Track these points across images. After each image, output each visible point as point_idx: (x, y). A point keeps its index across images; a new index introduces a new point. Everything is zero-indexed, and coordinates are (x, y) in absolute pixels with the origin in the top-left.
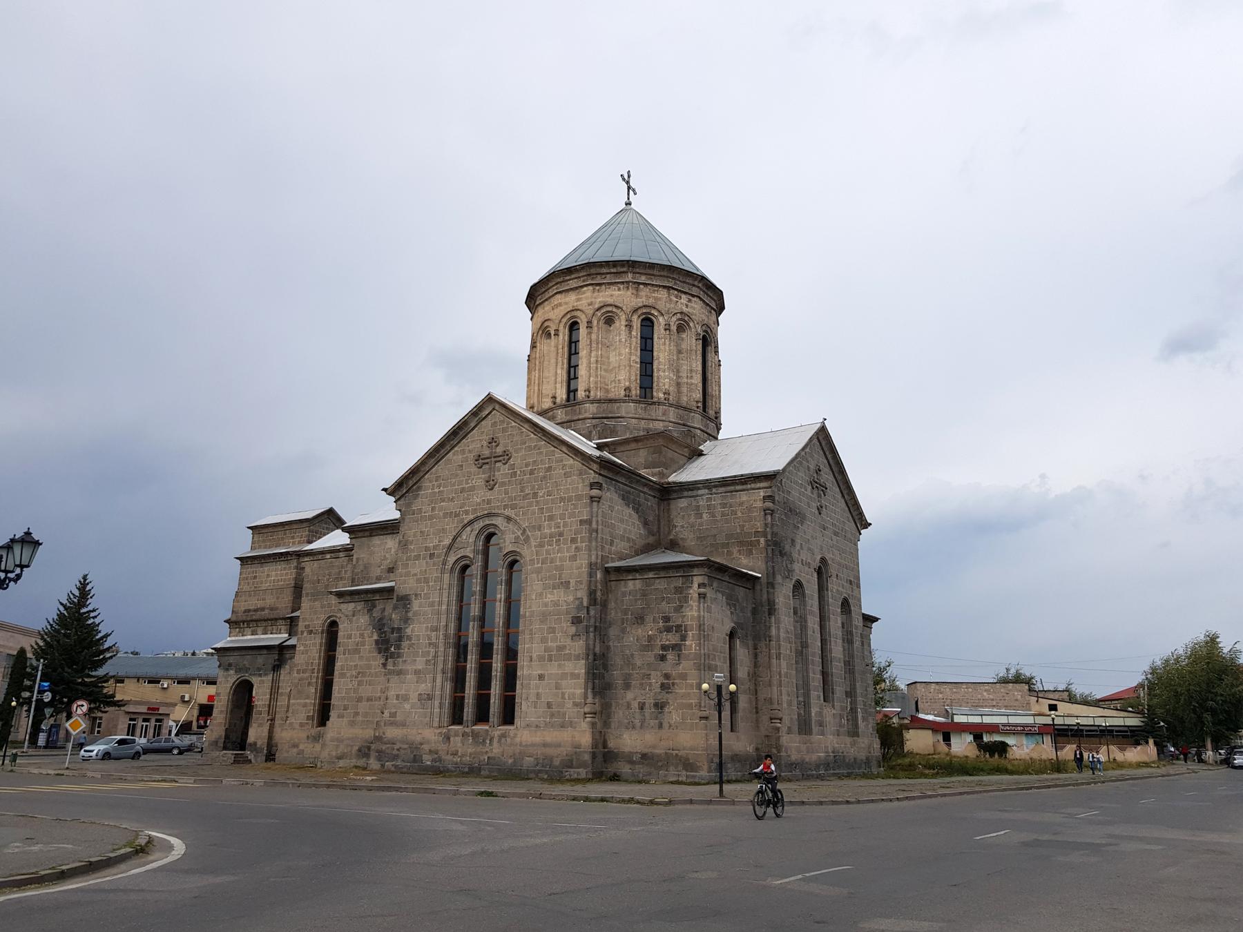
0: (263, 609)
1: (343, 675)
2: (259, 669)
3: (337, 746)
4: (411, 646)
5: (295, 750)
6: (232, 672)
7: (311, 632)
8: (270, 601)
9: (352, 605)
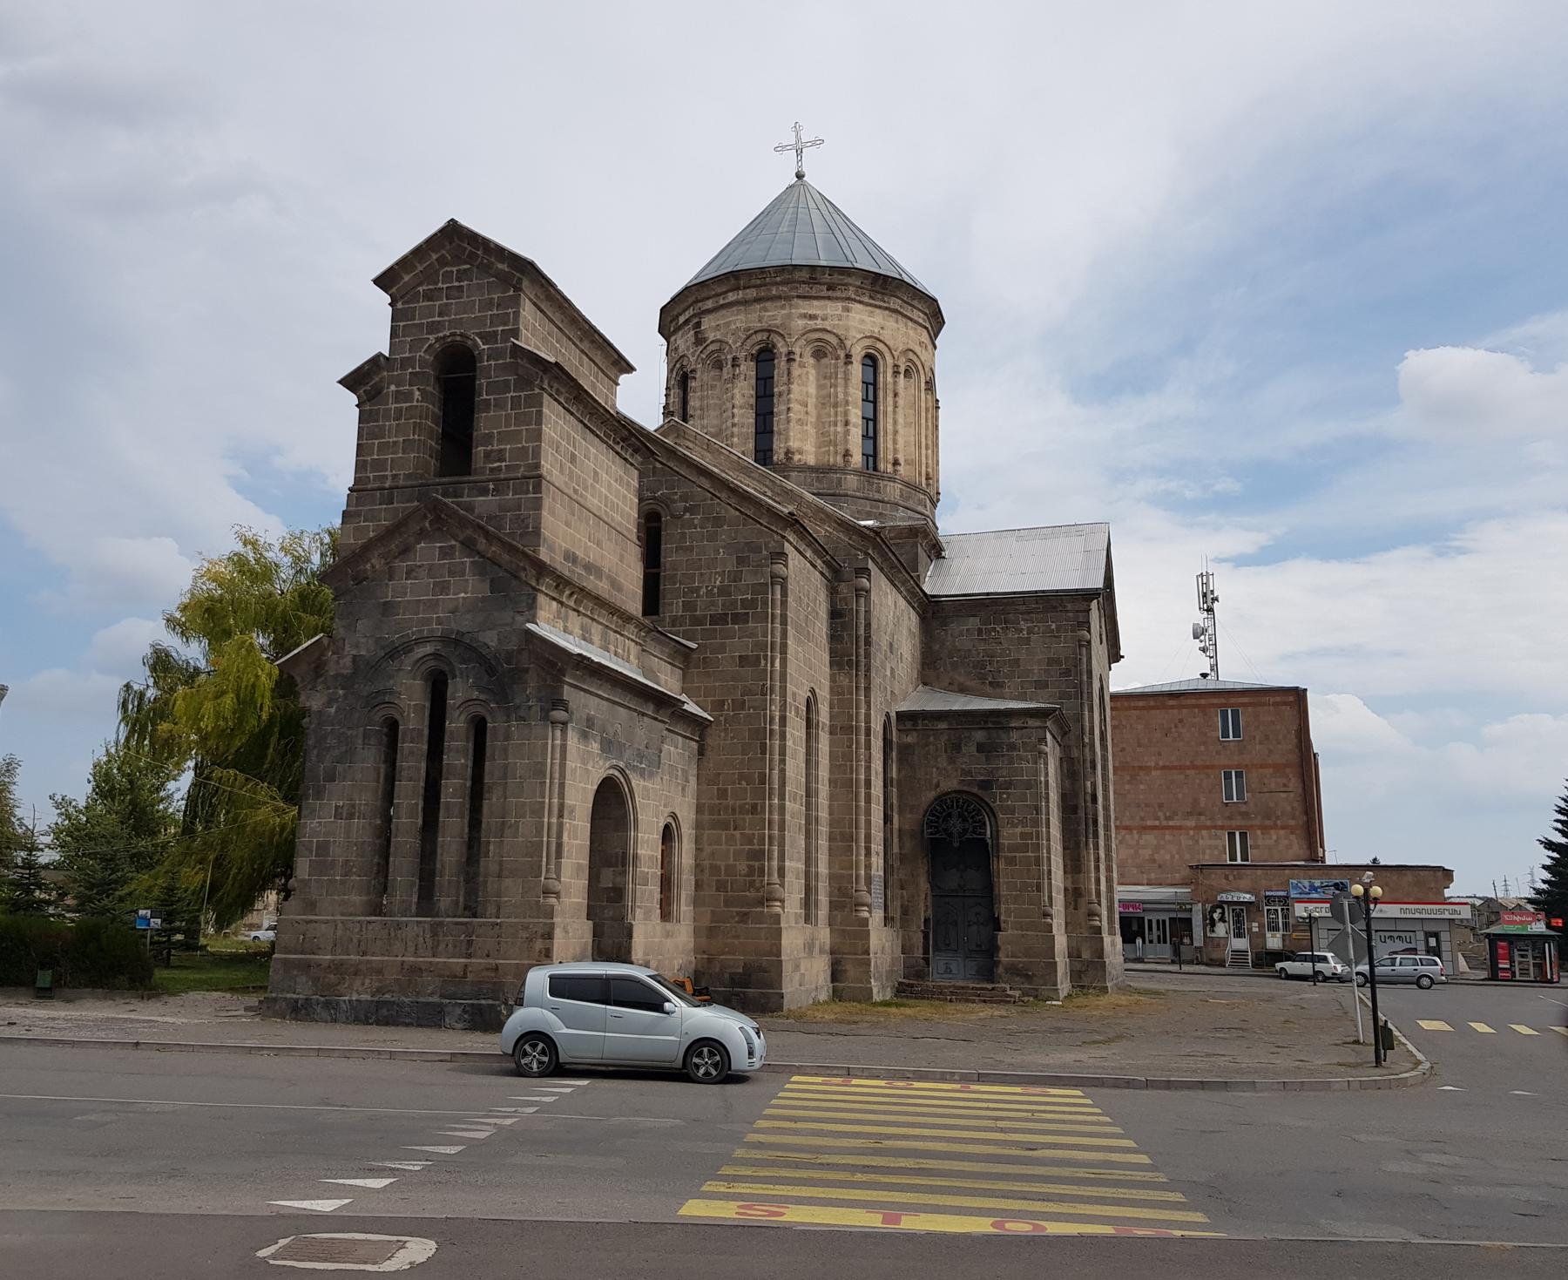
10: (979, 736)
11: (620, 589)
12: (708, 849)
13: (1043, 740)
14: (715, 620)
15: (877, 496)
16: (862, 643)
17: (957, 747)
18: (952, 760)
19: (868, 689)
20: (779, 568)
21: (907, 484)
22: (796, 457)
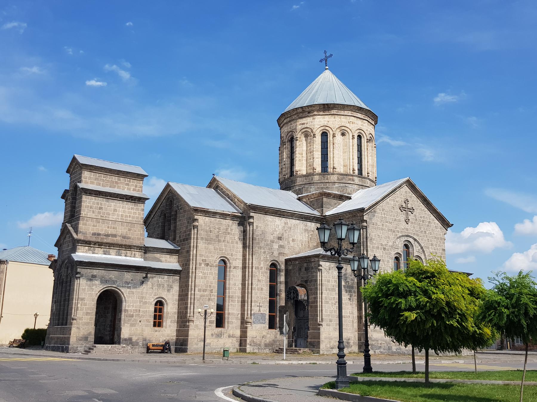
0: (115, 236)
1: (327, 302)
2: (128, 283)
3: (330, 342)
6: (97, 282)
7: (207, 265)
8: (121, 230)
9: (328, 264)
10: (305, 265)
14: (184, 240)
15: (326, 181)
17: (300, 269)
18: (299, 274)
20: (196, 224)
21: (342, 174)
22: (299, 173)
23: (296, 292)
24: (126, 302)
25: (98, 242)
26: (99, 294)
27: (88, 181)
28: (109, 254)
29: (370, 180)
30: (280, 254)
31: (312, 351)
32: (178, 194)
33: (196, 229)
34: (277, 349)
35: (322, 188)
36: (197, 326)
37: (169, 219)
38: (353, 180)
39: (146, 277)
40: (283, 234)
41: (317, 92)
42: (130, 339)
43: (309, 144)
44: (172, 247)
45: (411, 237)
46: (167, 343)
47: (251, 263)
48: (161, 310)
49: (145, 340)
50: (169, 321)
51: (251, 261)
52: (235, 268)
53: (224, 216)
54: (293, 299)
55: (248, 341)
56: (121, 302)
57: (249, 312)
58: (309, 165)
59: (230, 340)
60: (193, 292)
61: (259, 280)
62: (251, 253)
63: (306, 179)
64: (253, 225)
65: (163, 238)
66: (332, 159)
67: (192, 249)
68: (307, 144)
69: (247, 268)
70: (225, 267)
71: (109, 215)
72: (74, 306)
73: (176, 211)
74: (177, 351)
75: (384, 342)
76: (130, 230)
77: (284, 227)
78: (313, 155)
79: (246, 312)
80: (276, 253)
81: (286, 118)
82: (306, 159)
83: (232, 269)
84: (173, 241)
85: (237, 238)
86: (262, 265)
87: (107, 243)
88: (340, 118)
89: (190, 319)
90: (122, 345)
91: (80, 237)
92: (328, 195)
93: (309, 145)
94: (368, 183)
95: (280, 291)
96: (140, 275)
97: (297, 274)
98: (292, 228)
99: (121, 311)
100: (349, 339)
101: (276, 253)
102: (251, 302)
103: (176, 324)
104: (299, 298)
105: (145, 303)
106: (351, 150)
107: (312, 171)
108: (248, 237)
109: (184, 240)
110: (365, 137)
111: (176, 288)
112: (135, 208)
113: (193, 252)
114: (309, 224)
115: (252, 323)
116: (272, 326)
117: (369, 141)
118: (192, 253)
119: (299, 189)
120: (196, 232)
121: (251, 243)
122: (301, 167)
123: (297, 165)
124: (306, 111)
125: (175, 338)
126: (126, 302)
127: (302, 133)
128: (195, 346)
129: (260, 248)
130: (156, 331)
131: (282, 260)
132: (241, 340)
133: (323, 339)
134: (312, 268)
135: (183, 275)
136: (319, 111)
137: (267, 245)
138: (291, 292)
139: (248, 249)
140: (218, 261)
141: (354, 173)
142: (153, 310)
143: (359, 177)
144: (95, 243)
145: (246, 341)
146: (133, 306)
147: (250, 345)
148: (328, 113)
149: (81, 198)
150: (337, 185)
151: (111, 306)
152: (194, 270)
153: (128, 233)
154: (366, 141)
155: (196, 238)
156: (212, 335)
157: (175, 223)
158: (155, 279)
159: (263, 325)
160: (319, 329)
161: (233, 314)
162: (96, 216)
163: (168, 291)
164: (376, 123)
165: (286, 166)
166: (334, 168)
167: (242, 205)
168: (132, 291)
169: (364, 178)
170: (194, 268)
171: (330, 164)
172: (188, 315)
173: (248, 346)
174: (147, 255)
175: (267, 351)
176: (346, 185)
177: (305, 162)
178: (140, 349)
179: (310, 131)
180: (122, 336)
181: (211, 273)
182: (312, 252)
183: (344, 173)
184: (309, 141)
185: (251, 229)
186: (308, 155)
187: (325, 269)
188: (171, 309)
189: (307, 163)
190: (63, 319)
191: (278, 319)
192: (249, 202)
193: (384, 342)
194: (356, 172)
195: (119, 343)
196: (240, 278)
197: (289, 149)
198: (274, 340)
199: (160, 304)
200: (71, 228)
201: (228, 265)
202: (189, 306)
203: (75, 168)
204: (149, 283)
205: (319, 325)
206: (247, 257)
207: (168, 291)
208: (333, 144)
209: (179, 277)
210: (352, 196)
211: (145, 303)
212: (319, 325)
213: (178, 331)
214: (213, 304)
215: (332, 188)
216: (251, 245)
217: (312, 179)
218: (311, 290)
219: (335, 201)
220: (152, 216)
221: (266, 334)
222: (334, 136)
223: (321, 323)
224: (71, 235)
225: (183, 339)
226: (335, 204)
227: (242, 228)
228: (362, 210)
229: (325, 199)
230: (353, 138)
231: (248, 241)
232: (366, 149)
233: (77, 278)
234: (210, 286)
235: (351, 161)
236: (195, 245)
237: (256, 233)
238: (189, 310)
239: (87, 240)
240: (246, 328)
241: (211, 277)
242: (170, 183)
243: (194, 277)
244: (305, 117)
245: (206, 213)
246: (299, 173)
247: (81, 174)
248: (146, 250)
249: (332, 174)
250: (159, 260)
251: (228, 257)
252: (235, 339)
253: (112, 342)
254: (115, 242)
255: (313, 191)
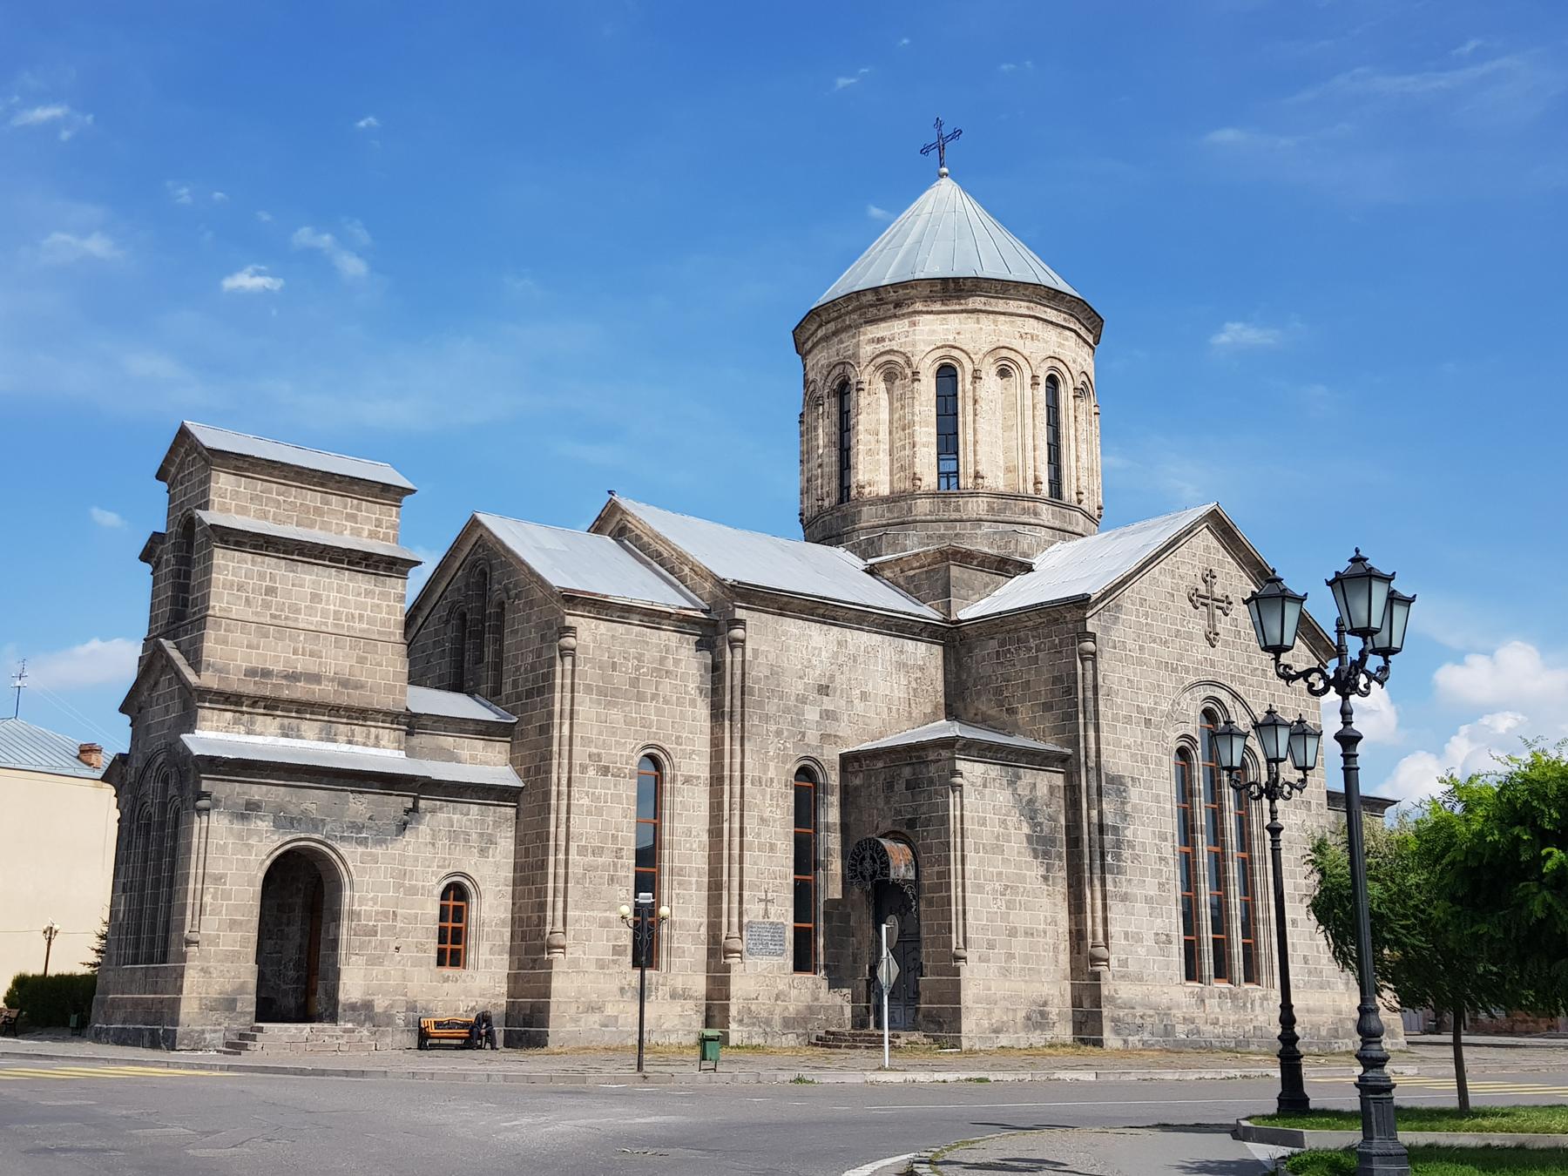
0: (315, 678)
1: (979, 888)
2: (359, 828)
3: (990, 1012)
4: (1135, 858)
5: (595, 1018)
7: (605, 771)
8: (335, 660)
10: (907, 772)
11: (359, 686)
12: (519, 902)
13: (955, 773)
14: (529, 694)
15: (955, 516)
16: (738, 693)
19: (742, 738)
20: (569, 641)
21: (1001, 496)
22: (866, 491)
23: (882, 857)
24: (352, 888)
25: (265, 698)
26: (268, 863)
27: (230, 503)
28: (299, 737)
29: (1084, 513)
30: (825, 737)
31: (936, 1040)
32: (508, 551)
33: (568, 660)
34: (822, 1033)
35: (942, 537)
36: (575, 963)
37: (480, 626)
38: (1036, 514)
39: (415, 809)
40: (832, 677)
41: (919, 242)
42: (368, 1006)
43: (899, 402)
44: (490, 716)
45: (1222, 686)
46: (484, 1018)
47: (737, 767)
48: (459, 915)
49: (412, 1007)
50: (485, 947)
51: (737, 760)
52: (687, 780)
53: (653, 617)
54: (872, 877)
55: (733, 1011)
56: (338, 887)
57: (735, 919)
58: (903, 467)
59: (677, 1007)
60: (561, 856)
61: (763, 820)
62: (737, 735)
63: (890, 510)
64: (743, 648)
65: (457, 687)
66: (970, 448)
67: (557, 721)
68: (891, 403)
69: (727, 781)
70: (659, 780)
71: (298, 611)
72: (190, 901)
73: (501, 604)
74: (512, 1042)
75: (1151, 1012)
76: (361, 660)
77: (835, 655)
78: (912, 435)
79: (725, 920)
80: (812, 737)
81: (824, 323)
82: (888, 446)
83: (679, 784)
84: (493, 696)
85: (692, 687)
86: (771, 773)
87: (292, 702)
88: (995, 322)
89: (555, 942)
90: (342, 1025)
91: (208, 680)
92: (965, 558)
93: (897, 405)
94: (1080, 523)
95: (827, 852)
96: (397, 803)
97: (881, 803)
98: (860, 659)
99: (336, 918)
100: (1045, 1004)
101: (812, 737)
102: (741, 889)
103: (506, 956)
104: (892, 875)
105: (412, 891)
106: (1029, 421)
107: (908, 485)
108: (728, 684)
109: (529, 694)
110: (1070, 382)
111: (506, 844)
112: (377, 590)
113: (561, 730)
114: (910, 645)
115: (745, 954)
116: (803, 962)
117: (1080, 393)
118: (556, 734)
119: (870, 542)
120: (568, 667)
121: (738, 703)
122: (873, 473)
123: (860, 467)
124: (890, 301)
125: (503, 1001)
126: (352, 888)
127: (878, 368)
128: (570, 1027)
129: (766, 718)
130: (446, 980)
131: (831, 756)
132: (708, 1008)
133: (970, 1004)
134: (931, 782)
135: (529, 804)
136: (927, 299)
137: (787, 710)
138: (864, 859)
139: (727, 723)
140: (637, 759)
141: (1037, 491)
142: (437, 912)
143: (1053, 504)
144: (255, 701)
145: (726, 1009)
146: (375, 900)
147: (741, 1021)
148: (957, 308)
149: (210, 556)
150: (986, 528)
151: (299, 901)
152: (564, 789)
153: (357, 672)
154: (1071, 393)
155: (568, 688)
156: (622, 989)
157: (501, 641)
158: (441, 816)
159: (776, 960)
160: (957, 972)
161: (683, 924)
162: (257, 614)
163: (483, 852)
164: (1097, 343)
165: (827, 470)
166: (977, 476)
167: (708, 585)
168: (371, 854)
169: (1068, 507)
170: (564, 781)
171: (966, 463)
172: (548, 928)
173: (733, 1026)
174: (416, 740)
175: (790, 1040)
176: (1016, 527)
177: (887, 458)
178: (398, 1037)
179: (901, 361)
180: (342, 997)
181: (617, 798)
182: (934, 730)
183: (1008, 491)
184: (897, 392)
185: (738, 658)
186: (896, 436)
187: (973, 784)
188: (491, 911)
189: (892, 461)
190: (152, 942)
191: (821, 941)
192: (730, 574)
193: (1151, 1012)
194: (1045, 488)
195: (333, 1019)
196: (704, 812)
197: (835, 418)
198: (809, 1008)
199: (456, 894)
200: (175, 654)
201: (667, 771)
202: (550, 899)
203: (186, 463)
204: (423, 830)
205: (958, 958)
206: (727, 747)
207: (483, 852)
208: (975, 401)
209: (513, 811)
210: (1036, 561)
211: (412, 891)
212: (958, 958)
213: (513, 979)
214: (623, 894)
215: (971, 536)
216: (738, 709)
217: (910, 509)
218: (929, 849)
219: (984, 577)
220: (420, 621)
221: (786, 988)
222: (976, 377)
223: (961, 953)
224: (178, 673)
225: (532, 1004)
226: (986, 586)
227: (707, 658)
228: (1081, 603)
229: (955, 571)
230: (1035, 384)
231: (728, 698)
232: (1072, 419)
233: (200, 811)
234: (614, 837)
235: (1030, 454)
236: (567, 708)
237: (752, 673)
238: (549, 913)
239: (228, 690)
240: (727, 968)
241: (618, 810)
242: (481, 517)
243: (564, 809)
244: (884, 319)
245: (600, 607)
246: (866, 491)
247: (207, 480)
248: (412, 724)
249: (971, 495)
250: (451, 757)
251: (666, 746)
252: (690, 1004)
253: (304, 1014)
254: (317, 698)
255: (914, 545)
